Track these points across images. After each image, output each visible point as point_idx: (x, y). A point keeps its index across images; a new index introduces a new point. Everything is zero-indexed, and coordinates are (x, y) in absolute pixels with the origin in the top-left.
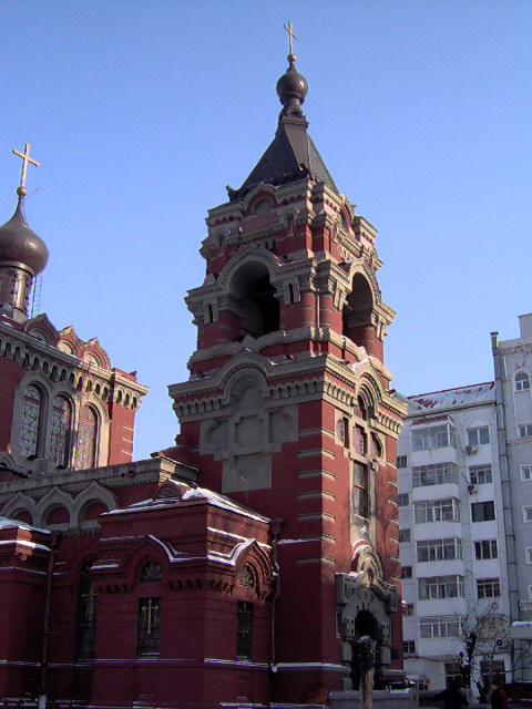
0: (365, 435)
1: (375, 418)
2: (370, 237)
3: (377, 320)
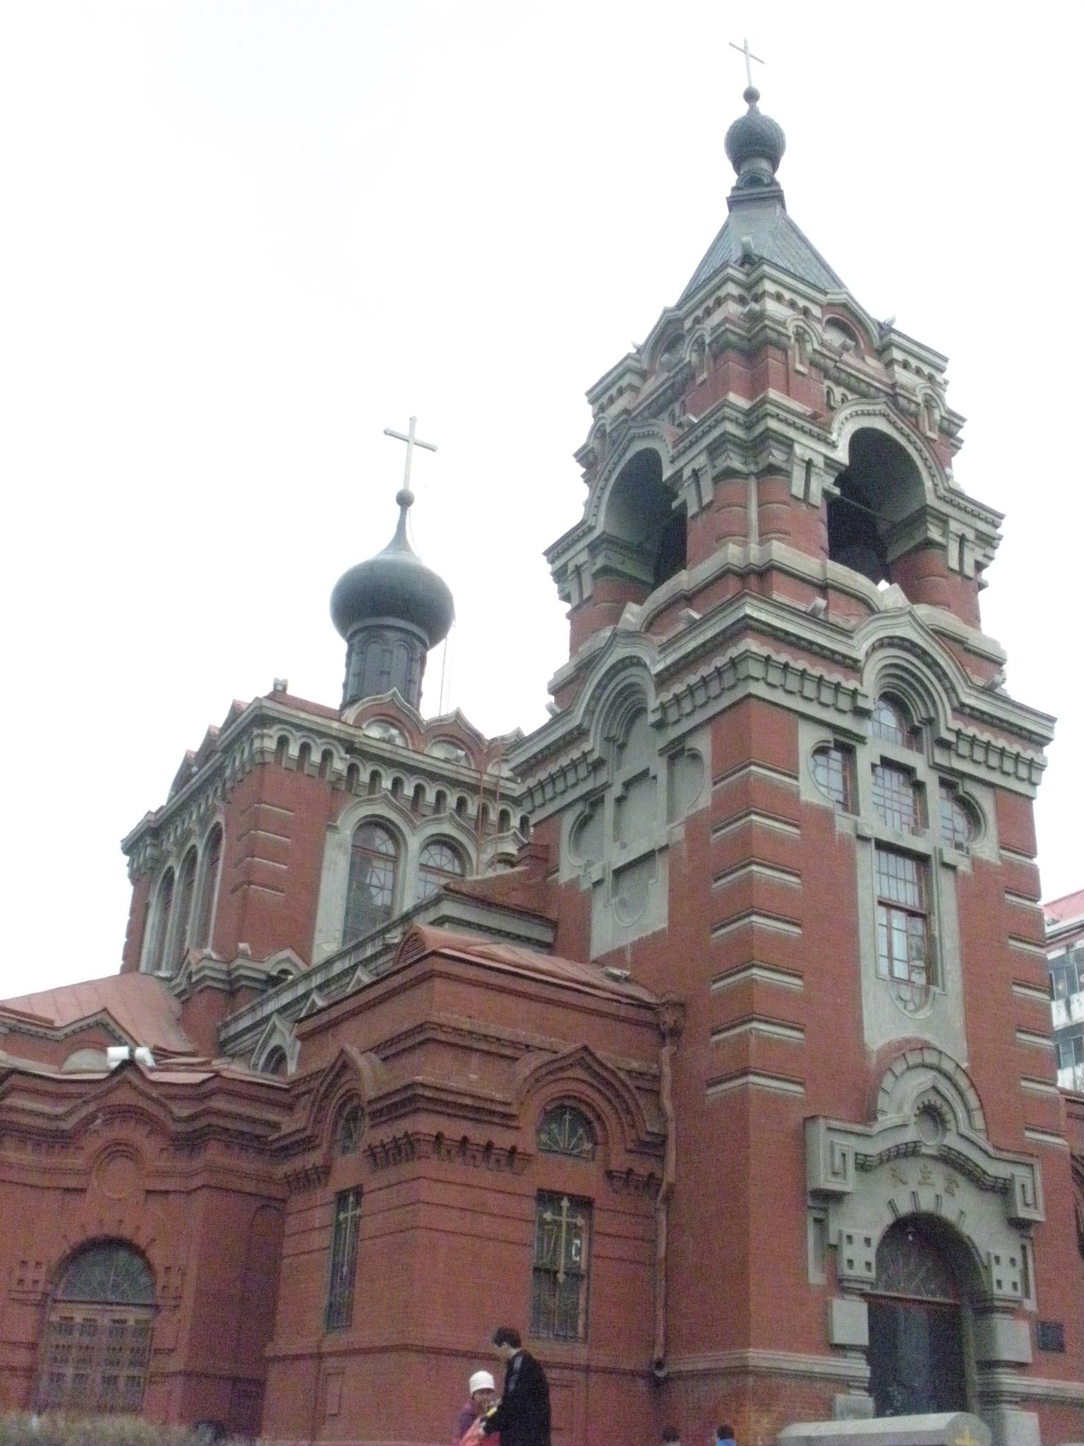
0: (919, 787)
1: (944, 744)
2: (927, 370)
3: (945, 532)
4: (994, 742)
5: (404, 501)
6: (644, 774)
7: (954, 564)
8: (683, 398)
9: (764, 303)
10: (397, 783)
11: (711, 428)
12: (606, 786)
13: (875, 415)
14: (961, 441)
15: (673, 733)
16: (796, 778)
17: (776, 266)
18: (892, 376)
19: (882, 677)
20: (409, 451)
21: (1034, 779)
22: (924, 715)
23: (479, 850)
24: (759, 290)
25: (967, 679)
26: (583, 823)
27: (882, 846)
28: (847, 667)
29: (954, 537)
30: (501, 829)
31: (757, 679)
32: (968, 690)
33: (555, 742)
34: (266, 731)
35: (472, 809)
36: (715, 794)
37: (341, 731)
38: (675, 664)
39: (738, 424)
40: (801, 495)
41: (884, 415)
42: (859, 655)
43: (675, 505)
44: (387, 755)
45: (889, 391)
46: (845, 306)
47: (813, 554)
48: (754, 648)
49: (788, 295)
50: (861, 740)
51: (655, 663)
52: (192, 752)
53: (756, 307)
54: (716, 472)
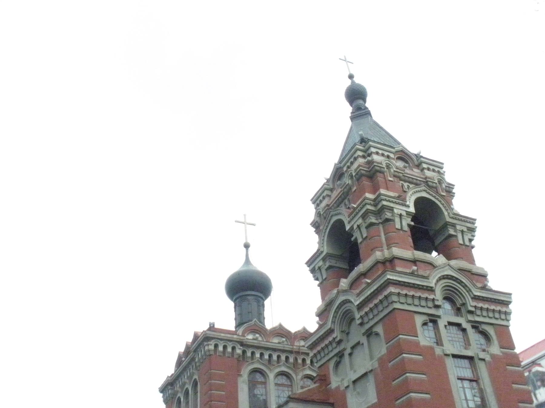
0: (464, 330)
2: (437, 169)
3: (456, 230)
4: (490, 308)
5: (247, 246)
6: (358, 343)
7: (461, 242)
8: (348, 197)
9: (372, 157)
10: (262, 355)
11: (362, 208)
12: (344, 349)
13: (421, 191)
14: (454, 193)
15: (367, 326)
16: (417, 337)
17: (374, 142)
18: (424, 175)
19: (442, 292)
20: (246, 227)
21: (508, 319)
22: (461, 302)
23: (296, 376)
24: (369, 152)
25: (474, 285)
26: (337, 364)
27: (455, 356)
28: (429, 290)
29: (459, 231)
30: (303, 366)
31: (396, 302)
32: (476, 290)
33: (322, 335)
34: (209, 343)
35: (291, 360)
36: (387, 348)
37: (238, 338)
38: (364, 300)
39: (371, 205)
40: (399, 228)
41: (425, 191)
42: (432, 285)
43: (353, 239)
44: (256, 345)
45: (424, 180)
46: (402, 151)
47: (407, 249)
48: (393, 291)
49: (380, 152)
50: (439, 317)
51: (356, 301)
52: (181, 352)
53: (369, 158)
54: (366, 224)
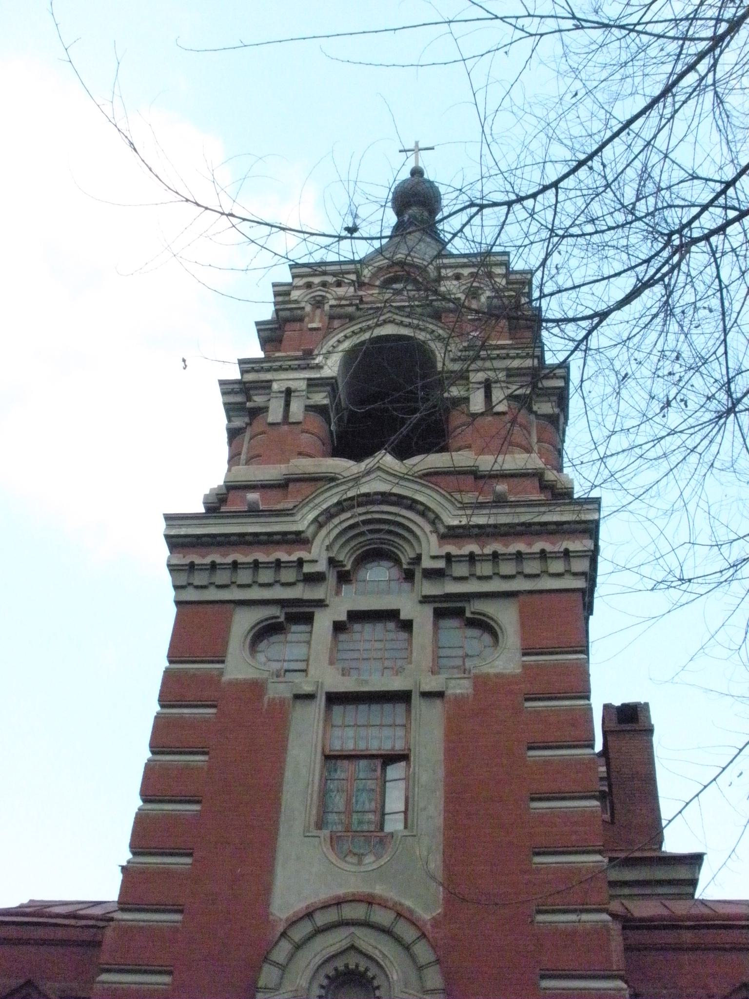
16: (223, 662)
41: (390, 322)
